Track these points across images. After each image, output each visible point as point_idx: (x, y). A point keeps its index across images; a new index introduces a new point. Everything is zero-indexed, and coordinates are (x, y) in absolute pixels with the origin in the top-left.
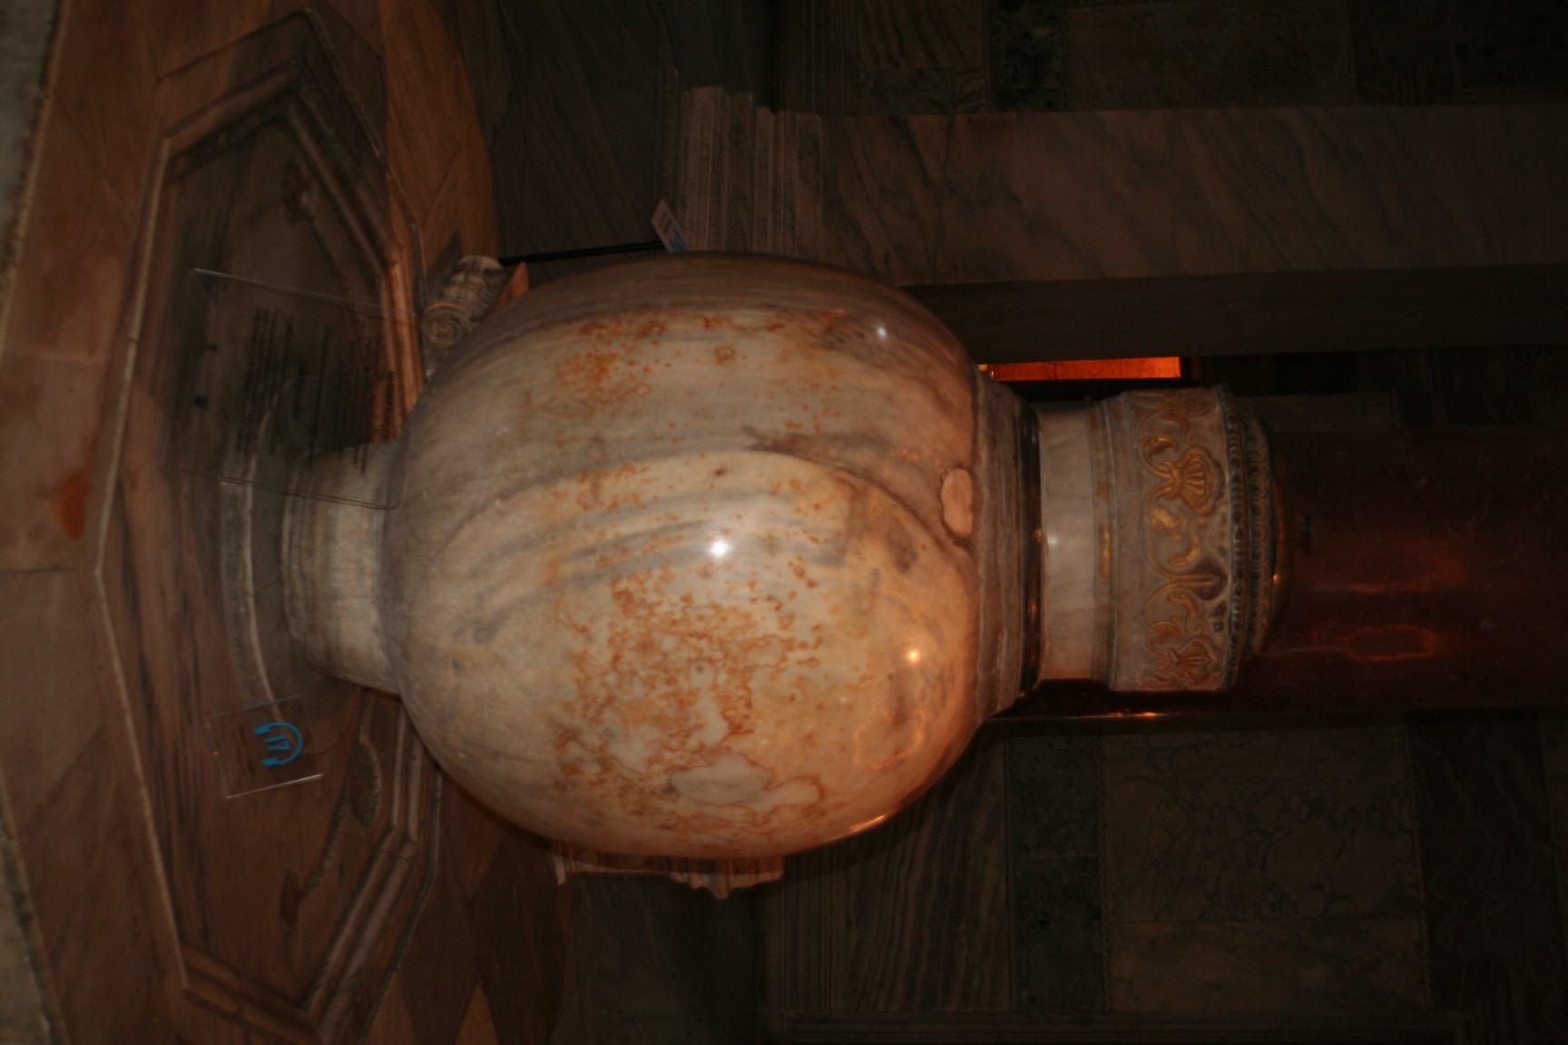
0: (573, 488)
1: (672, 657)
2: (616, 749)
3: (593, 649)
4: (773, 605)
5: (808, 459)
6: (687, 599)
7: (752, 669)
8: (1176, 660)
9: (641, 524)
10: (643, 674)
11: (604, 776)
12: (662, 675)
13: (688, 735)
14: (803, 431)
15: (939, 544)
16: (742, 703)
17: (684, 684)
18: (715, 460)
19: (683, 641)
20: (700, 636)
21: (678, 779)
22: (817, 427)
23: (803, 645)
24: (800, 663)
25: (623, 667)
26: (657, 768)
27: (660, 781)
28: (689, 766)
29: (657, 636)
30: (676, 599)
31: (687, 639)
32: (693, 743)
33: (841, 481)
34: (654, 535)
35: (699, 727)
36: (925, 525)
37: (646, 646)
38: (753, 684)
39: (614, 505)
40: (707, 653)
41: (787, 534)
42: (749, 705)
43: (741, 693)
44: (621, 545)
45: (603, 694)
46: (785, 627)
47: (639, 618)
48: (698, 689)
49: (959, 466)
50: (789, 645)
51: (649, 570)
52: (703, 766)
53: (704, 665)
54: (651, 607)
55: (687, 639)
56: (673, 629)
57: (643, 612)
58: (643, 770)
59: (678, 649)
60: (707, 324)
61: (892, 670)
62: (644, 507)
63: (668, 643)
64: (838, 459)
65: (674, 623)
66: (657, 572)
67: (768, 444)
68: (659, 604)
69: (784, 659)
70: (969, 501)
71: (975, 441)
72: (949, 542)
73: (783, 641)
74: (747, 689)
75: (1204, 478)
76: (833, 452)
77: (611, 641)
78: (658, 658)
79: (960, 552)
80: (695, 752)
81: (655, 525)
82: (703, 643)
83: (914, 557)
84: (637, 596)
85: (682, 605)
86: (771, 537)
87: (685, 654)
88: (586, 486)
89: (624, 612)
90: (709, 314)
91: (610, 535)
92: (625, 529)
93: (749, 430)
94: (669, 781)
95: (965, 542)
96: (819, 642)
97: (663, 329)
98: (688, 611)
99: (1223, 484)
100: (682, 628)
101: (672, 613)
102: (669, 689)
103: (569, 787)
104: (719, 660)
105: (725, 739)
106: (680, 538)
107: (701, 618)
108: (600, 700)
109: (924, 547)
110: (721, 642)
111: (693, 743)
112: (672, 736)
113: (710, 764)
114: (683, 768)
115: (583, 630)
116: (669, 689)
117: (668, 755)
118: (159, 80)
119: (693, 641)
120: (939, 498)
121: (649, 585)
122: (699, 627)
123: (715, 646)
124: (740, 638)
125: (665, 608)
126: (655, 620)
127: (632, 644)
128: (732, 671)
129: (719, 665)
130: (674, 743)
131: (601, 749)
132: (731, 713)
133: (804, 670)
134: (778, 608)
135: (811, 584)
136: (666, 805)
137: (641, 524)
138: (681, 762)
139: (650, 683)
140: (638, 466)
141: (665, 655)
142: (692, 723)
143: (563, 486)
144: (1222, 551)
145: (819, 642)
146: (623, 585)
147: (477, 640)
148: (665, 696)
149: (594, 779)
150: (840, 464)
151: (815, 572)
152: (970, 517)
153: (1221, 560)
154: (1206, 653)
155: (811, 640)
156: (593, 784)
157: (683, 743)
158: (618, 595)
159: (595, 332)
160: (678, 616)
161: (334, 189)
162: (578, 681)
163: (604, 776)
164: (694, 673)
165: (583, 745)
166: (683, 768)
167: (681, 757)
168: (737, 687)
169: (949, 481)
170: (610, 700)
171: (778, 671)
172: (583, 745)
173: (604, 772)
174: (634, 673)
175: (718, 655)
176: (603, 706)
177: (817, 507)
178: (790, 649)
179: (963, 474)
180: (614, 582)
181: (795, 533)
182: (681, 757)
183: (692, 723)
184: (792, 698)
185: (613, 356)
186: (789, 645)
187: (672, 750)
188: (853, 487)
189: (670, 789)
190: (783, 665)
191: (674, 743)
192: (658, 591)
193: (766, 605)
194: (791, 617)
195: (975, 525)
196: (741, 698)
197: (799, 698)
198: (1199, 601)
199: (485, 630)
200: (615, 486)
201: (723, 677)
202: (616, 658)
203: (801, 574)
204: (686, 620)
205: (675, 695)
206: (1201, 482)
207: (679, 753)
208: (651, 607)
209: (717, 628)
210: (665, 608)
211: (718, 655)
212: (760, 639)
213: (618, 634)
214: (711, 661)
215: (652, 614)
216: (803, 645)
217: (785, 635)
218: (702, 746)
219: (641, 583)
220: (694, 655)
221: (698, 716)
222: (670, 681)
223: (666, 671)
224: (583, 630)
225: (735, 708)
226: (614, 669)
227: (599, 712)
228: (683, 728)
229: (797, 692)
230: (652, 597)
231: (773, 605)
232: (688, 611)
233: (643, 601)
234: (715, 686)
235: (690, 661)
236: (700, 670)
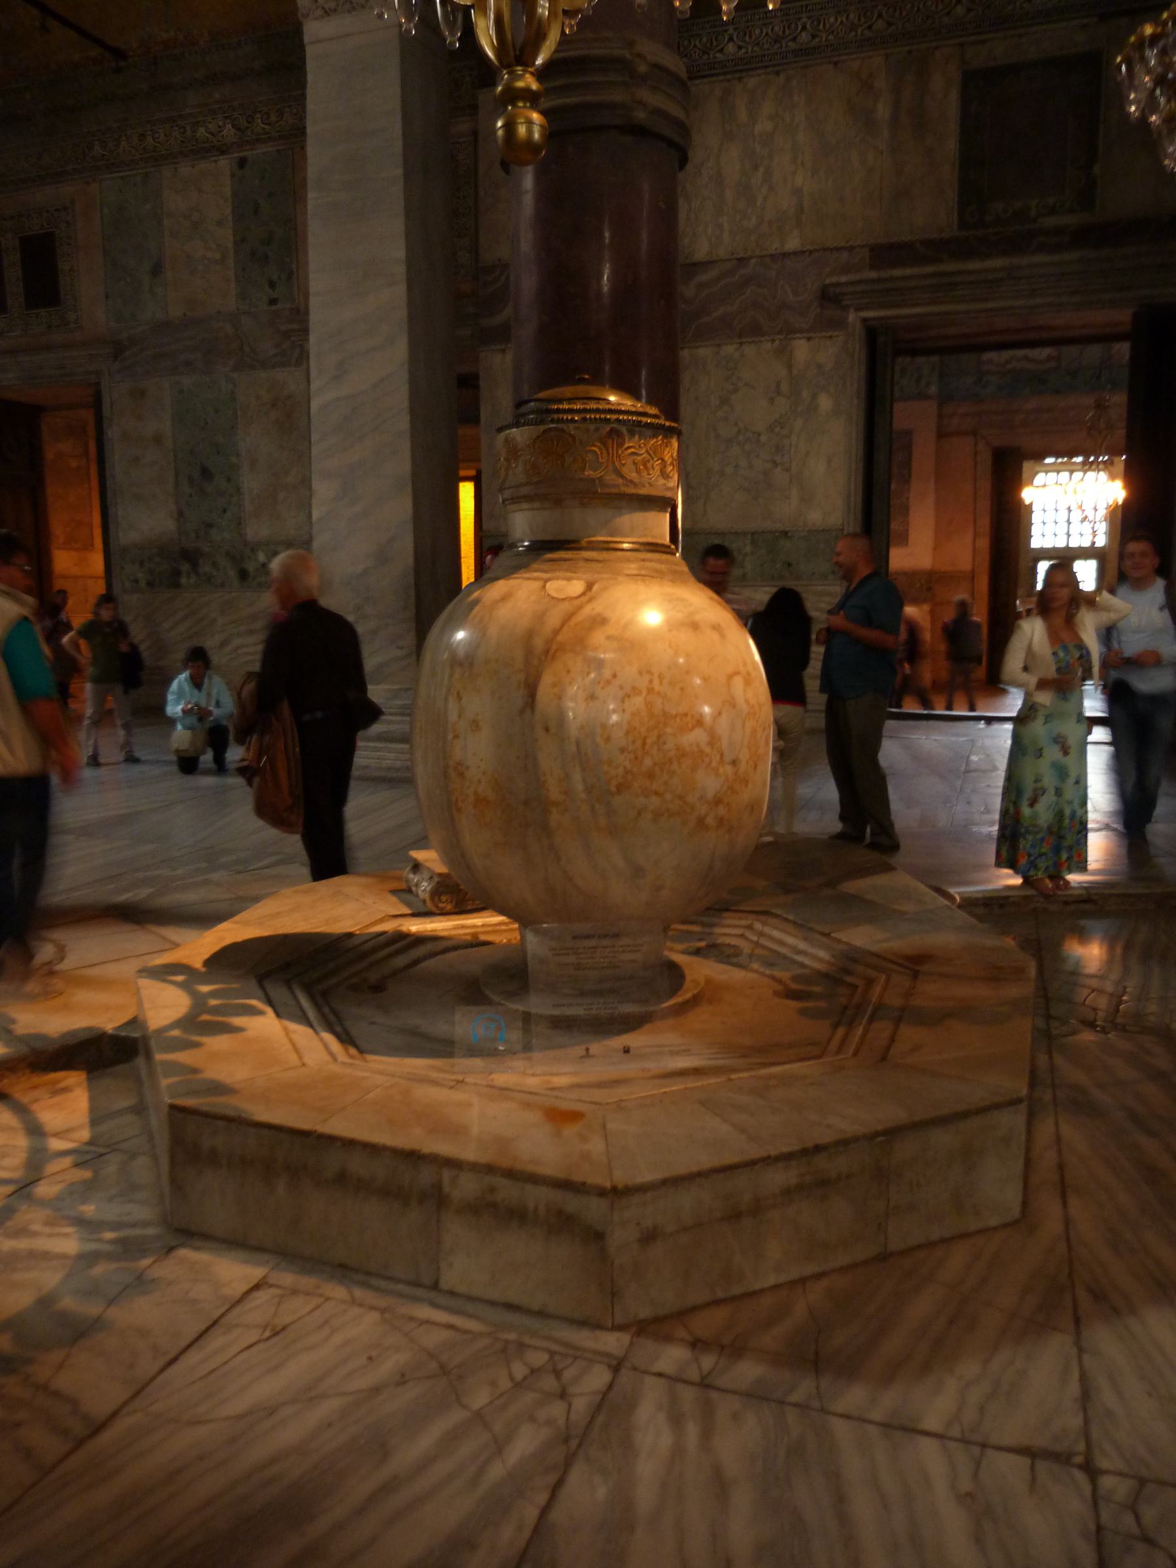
0: (555, 816)
2: (710, 794)
6: (622, 750)
8: (660, 461)
9: (577, 777)
15: (590, 600)
17: (672, 754)
20: (644, 743)
21: (728, 759)
23: (651, 681)
24: (661, 683)
26: (721, 771)
27: (729, 769)
33: (554, 657)
34: (583, 770)
35: (698, 745)
36: (580, 607)
37: (650, 775)
38: (674, 712)
39: (566, 793)
40: (654, 739)
41: (584, 690)
42: (686, 715)
43: (678, 720)
44: (589, 790)
46: (641, 692)
48: (676, 745)
49: (544, 587)
50: (650, 690)
54: (627, 772)
60: (456, 737)
63: (648, 762)
65: (636, 758)
66: (606, 768)
68: (625, 768)
69: (659, 693)
71: (528, 579)
72: (589, 594)
77: (646, 797)
79: (595, 587)
80: (713, 748)
82: (649, 741)
83: (599, 615)
86: (586, 700)
88: (554, 810)
90: (450, 736)
91: (583, 796)
93: (522, 712)
94: (729, 764)
95: (589, 586)
97: (459, 764)
99: (556, 428)
105: (705, 730)
106: (586, 754)
107: (634, 742)
109: (593, 609)
111: (707, 750)
112: (703, 761)
114: (722, 755)
115: (639, 813)
117: (714, 764)
118: (304, 1065)
119: (647, 747)
120: (563, 599)
122: (639, 743)
125: (627, 763)
126: (635, 769)
128: (665, 725)
132: (690, 726)
133: (665, 681)
135: (615, 676)
136: (743, 767)
137: (577, 777)
141: (655, 764)
144: (597, 430)
145: (649, 672)
146: (613, 789)
150: (543, 658)
151: (607, 673)
152: (574, 582)
157: (707, 755)
159: (460, 804)
160: (632, 756)
161: (364, 964)
164: (666, 747)
165: (706, 815)
169: (554, 594)
172: (706, 815)
174: (666, 783)
177: (568, 672)
178: (653, 689)
179: (548, 584)
184: (682, 689)
185: (475, 793)
186: (650, 690)
187: (711, 762)
189: (734, 763)
191: (707, 760)
194: (634, 688)
195: (578, 579)
196: (681, 719)
198: (626, 445)
199: (638, 872)
200: (554, 794)
201: (669, 730)
202: (656, 793)
203: (608, 682)
208: (627, 772)
209: (640, 733)
211: (656, 733)
214: (659, 737)
216: (651, 681)
217: (645, 692)
220: (656, 747)
221: (691, 745)
222: (670, 761)
224: (639, 813)
225: (687, 723)
230: (621, 771)
232: (630, 749)
235: (659, 750)
236: (665, 743)
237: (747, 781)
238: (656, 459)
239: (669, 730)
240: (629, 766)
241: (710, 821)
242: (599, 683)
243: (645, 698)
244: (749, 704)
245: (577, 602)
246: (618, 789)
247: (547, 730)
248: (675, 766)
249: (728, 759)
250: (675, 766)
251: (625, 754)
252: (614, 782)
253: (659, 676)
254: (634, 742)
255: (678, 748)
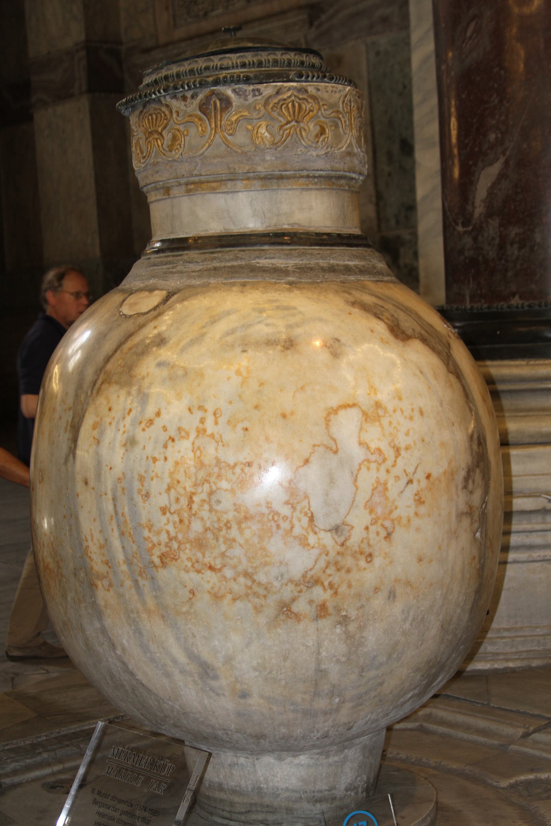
1: (208, 524)
3: (208, 587)
4: (170, 444)
5: (84, 416)
6: (164, 510)
7: (218, 461)
10: (223, 548)
11: (326, 584)
12: (223, 532)
13: (277, 514)
14: (70, 420)
16: (247, 469)
17: (230, 516)
18: (79, 487)
19: (195, 515)
20: (191, 501)
22: (70, 409)
23: (202, 421)
24: (216, 423)
25: (218, 564)
26: (312, 539)
27: (328, 539)
28: (310, 515)
29: (192, 536)
30: (164, 519)
31: (193, 512)
32: (286, 511)
34: (122, 534)
39: (107, 563)
40: (204, 496)
43: (238, 470)
45: (242, 580)
46: (188, 434)
47: (179, 548)
50: (201, 432)
51: (145, 539)
52: (309, 503)
53: (214, 498)
55: (193, 512)
56: (186, 522)
57: (175, 545)
58: (315, 552)
59: (202, 519)
61: (238, 350)
62: (106, 540)
63: (197, 527)
64: (87, 393)
65: (181, 521)
66: (146, 533)
67: (73, 446)
68: (168, 532)
69: (212, 436)
70: (147, 293)
73: (197, 436)
74: (235, 465)
75: (151, 115)
76: (83, 397)
77: (199, 572)
78: (209, 535)
80: (294, 508)
81: (116, 533)
82: (196, 498)
84: (164, 549)
85: (168, 514)
87: (205, 514)
89: (176, 560)
92: (120, 556)
93: (66, 461)
96: (201, 408)
98: (172, 511)
100: (186, 515)
101: (174, 523)
102: (235, 527)
103: (344, 613)
104: (211, 487)
107: (177, 500)
108: (249, 583)
110: (195, 485)
111: (286, 511)
112: (278, 527)
113: (306, 497)
114: (312, 519)
116: (235, 527)
117: (297, 531)
119: (195, 507)
121: (155, 540)
122: (184, 502)
123: (200, 489)
124: (193, 470)
125: (170, 528)
126: (180, 536)
127: (199, 555)
128: (219, 476)
129: (214, 488)
130: (285, 525)
131: (296, 585)
133: (222, 420)
134: (173, 440)
135: (158, 414)
137: (116, 543)
138: (305, 521)
139: (231, 542)
140: (85, 544)
141: (206, 530)
142: (266, 511)
143: (101, 603)
145: (201, 408)
146: (157, 561)
147: (216, 677)
148: (241, 531)
149: (330, 592)
153: (201, 96)
154: (285, 100)
155: (199, 414)
156: (336, 593)
157: (285, 518)
158: (164, 564)
160: (176, 518)
162: (234, 600)
163: (326, 584)
165: (294, 600)
166: (312, 519)
167: (300, 521)
168: (234, 473)
170: (246, 574)
171: (222, 441)
173: (322, 584)
174: (223, 555)
175: (206, 487)
176: (254, 581)
177: (110, 409)
178: (205, 431)
180: (155, 566)
181: (124, 426)
182: (300, 521)
183: (266, 511)
186: (201, 432)
188: (102, 383)
190: (217, 436)
191: (285, 525)
192: (159, 533)
193: (170, 449)
196: (242, 470)
197: (246, 424)
201: (224, 484)
202: (211, 568)
203: (151, 422)
204: (178, 512)
205: (239, 523)
206: (154, 116)
207: (295, 521)
209: (185, 488)
210: (170, 528)
212: (195, 454)
213: (193, 566)
214: (211, 493)
215: (175, 538)
217: (193, 435)
218: (287, 503)
219: (154, 545)
220: (206, 507)
221: (259, 505)
223: (220, 529)
226: (220, 570)
227: (259, 584)
228: (270, 517)
229: (240, 426)
230: (164, 538)
231: (170, 444)
233: (167, 545)
234: (233, 491)
235: (211, 510)
237: (370, 555)
238: (284, 121)
239: (224, 484)
240: (173, 534)
241: (300, 606)
242: (141, 423)
243: (193, 443)
244: (368, 448)
245: (141, 320)
246: (162, 562)
247: (86, 483)
248: (234, 532)
249: (321, 523)
250: (234, 532)
251: (168, 514)
252: (157, 552)
253: (215, 414)
254: (177, 500)
255: (237, 509)
